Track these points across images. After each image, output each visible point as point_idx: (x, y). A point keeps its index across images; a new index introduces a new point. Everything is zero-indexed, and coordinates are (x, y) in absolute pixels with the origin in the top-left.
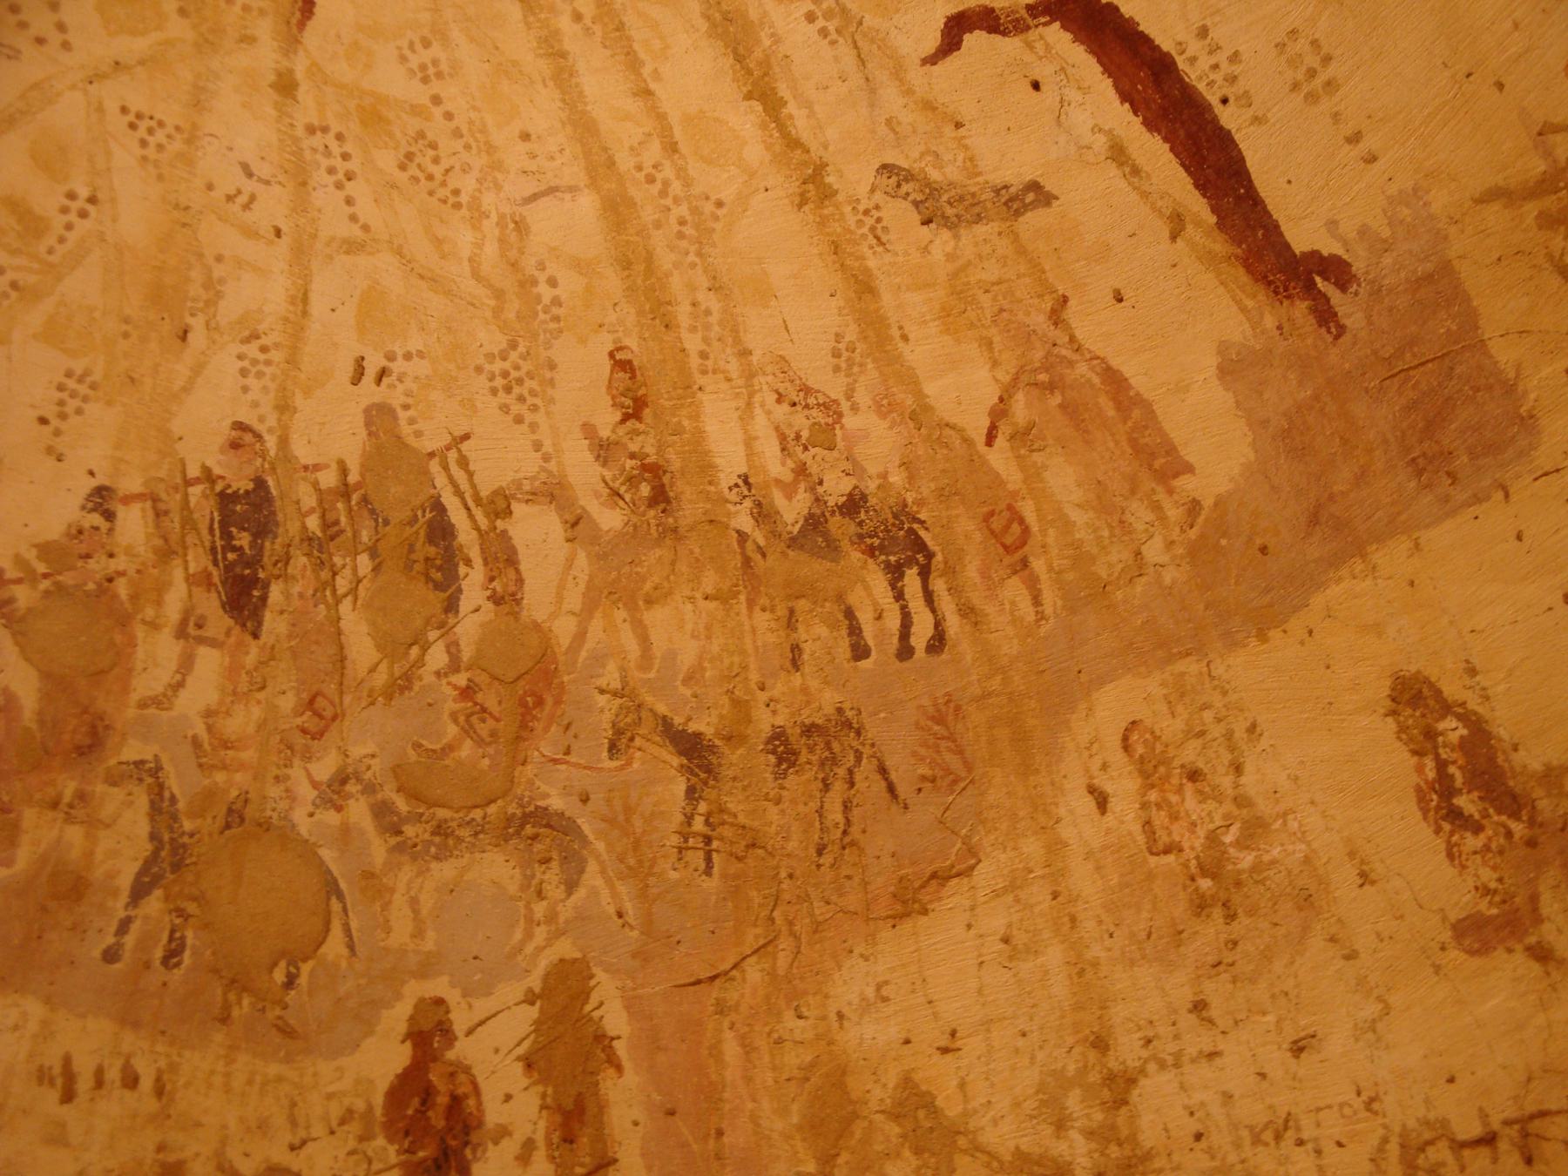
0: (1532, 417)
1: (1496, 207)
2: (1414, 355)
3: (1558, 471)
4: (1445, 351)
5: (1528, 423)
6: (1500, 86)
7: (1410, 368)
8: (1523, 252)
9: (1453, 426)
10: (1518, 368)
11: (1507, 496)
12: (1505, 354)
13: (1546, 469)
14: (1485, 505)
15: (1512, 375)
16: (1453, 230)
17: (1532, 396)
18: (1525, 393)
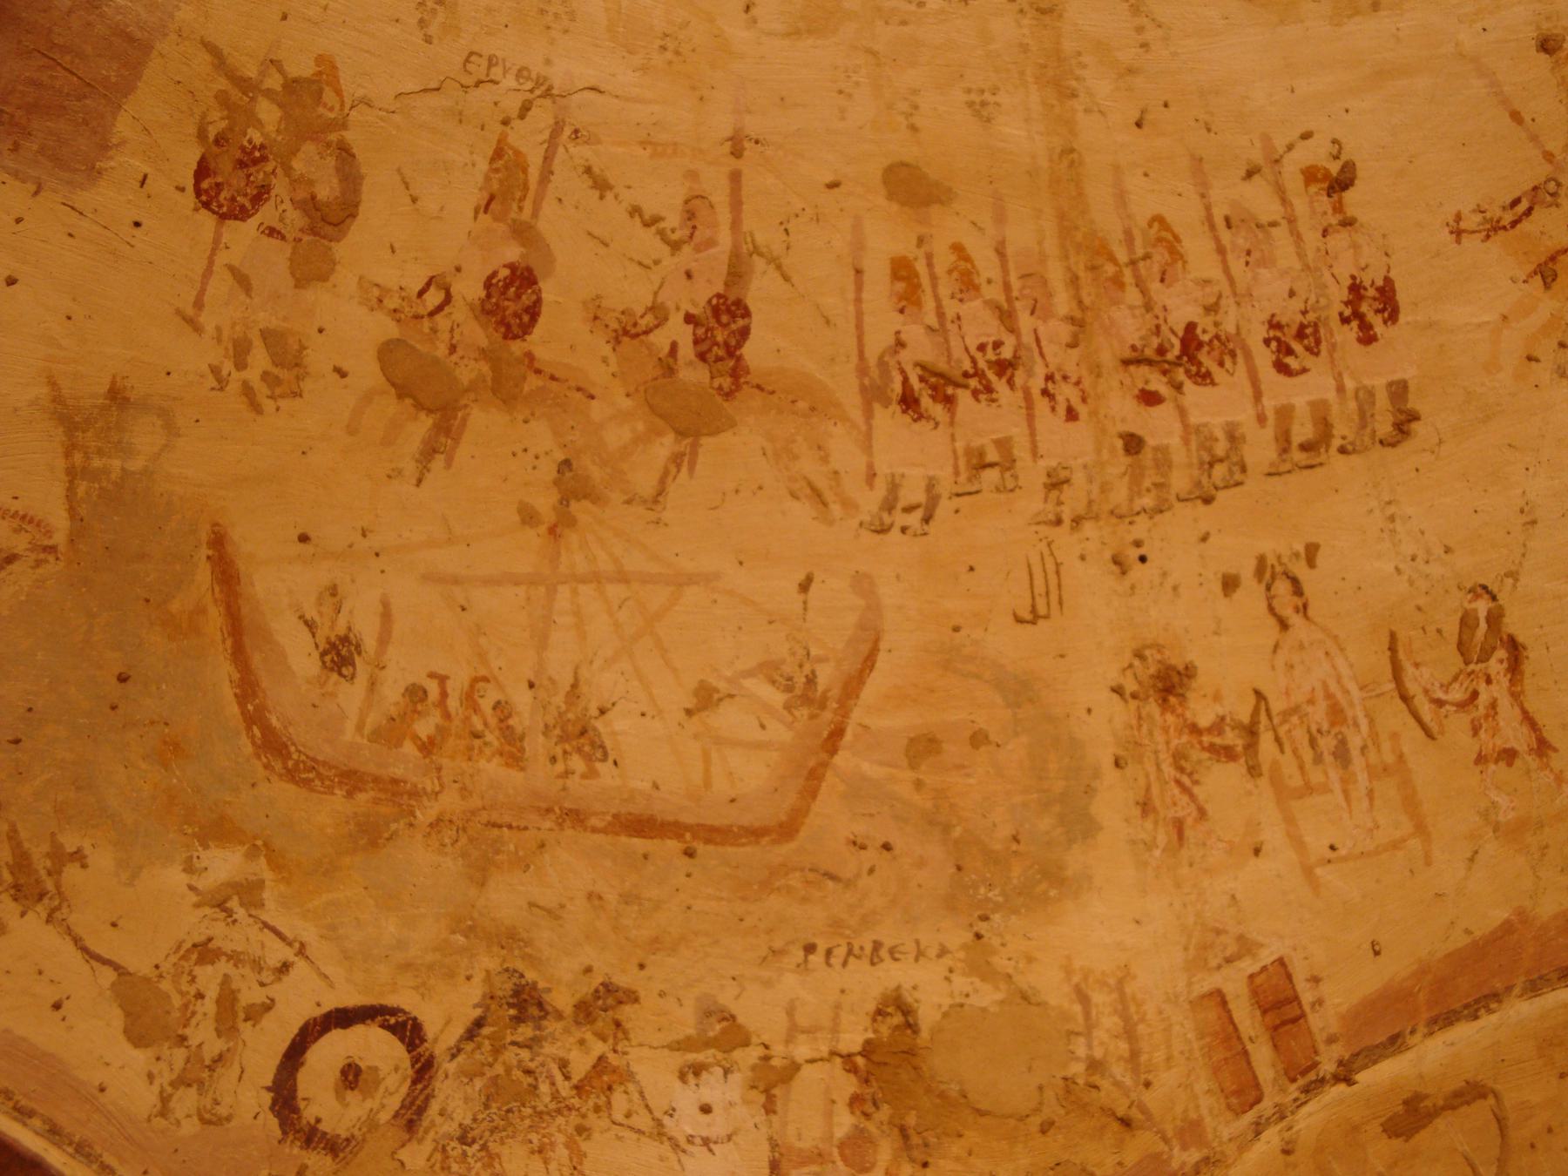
0: (99, 173)
1: (208, 58)
2: (72, 62)
3: (81, 213)
4: (92, 83)
5: (94, 173)
6: (284, 17)
7: (60, 64)
8: (194, 96)
9: (49, 124)
10: (123, 142)
11: (36, 193)
12: (123, 126)
13: (76, 206)
14: (17, 183)
15: (114, 141)
16: (173, 36)
17: (112, 164)
18: (111, 158)
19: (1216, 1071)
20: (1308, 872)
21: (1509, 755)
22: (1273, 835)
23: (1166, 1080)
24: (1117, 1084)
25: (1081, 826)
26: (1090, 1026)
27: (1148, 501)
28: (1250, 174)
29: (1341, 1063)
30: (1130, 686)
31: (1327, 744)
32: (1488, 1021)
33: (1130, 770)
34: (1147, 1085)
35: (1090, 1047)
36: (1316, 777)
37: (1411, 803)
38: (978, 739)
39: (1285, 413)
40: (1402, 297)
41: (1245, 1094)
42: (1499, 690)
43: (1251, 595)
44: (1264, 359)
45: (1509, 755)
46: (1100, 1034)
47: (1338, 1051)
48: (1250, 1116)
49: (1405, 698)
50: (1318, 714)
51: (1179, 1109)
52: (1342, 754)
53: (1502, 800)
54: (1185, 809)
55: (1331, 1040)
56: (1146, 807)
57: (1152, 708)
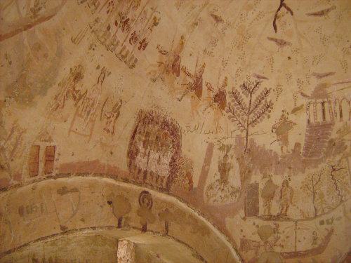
19: (30, 164)
20: (70, 131)
21: (108, 131)
22: (69, 120)
23: (18, 161)
24: (5, 157)
25: (43, 92)
26: (9, 138)
27: (102, 40)
28: (152, 9)
29: (57, 175)
30: (73, 71)
31: (88, 110)
32: (85, 177)
33: (60, 87)
34: (12, 160)
35: (5, 144)
36: (83, 114)
37: (92, 130)
38: (45, 56)
39: (124, 48)
40: (147, 48)
41: (34, 173)
42: (113, 119)
43: (99, 71)
44: (130, 36)
45: (108, 131)
46: (9, 142)
47: (57, 172)
48: (34, 178)
49: (102, 110)
50: (91, 102)
51: (17, 170)
52: (89, 113)
53: (104, 138)
54: (61, 103)
55: (57, 169)
56: (56, 98)
57: (72, 78)
